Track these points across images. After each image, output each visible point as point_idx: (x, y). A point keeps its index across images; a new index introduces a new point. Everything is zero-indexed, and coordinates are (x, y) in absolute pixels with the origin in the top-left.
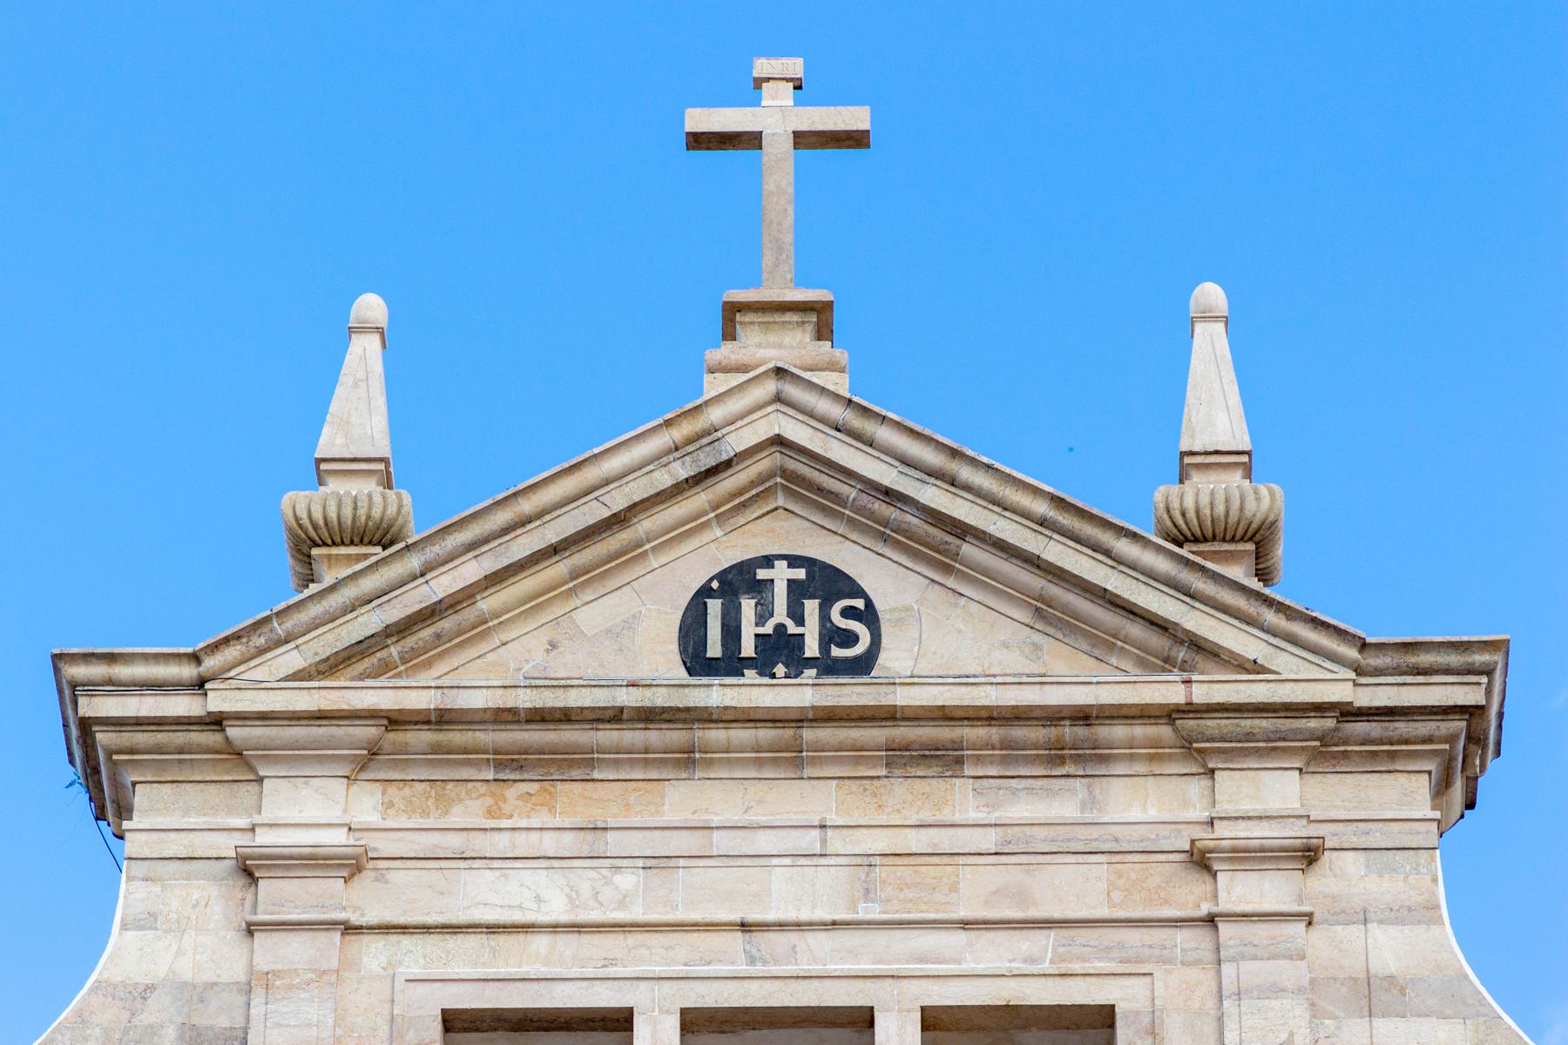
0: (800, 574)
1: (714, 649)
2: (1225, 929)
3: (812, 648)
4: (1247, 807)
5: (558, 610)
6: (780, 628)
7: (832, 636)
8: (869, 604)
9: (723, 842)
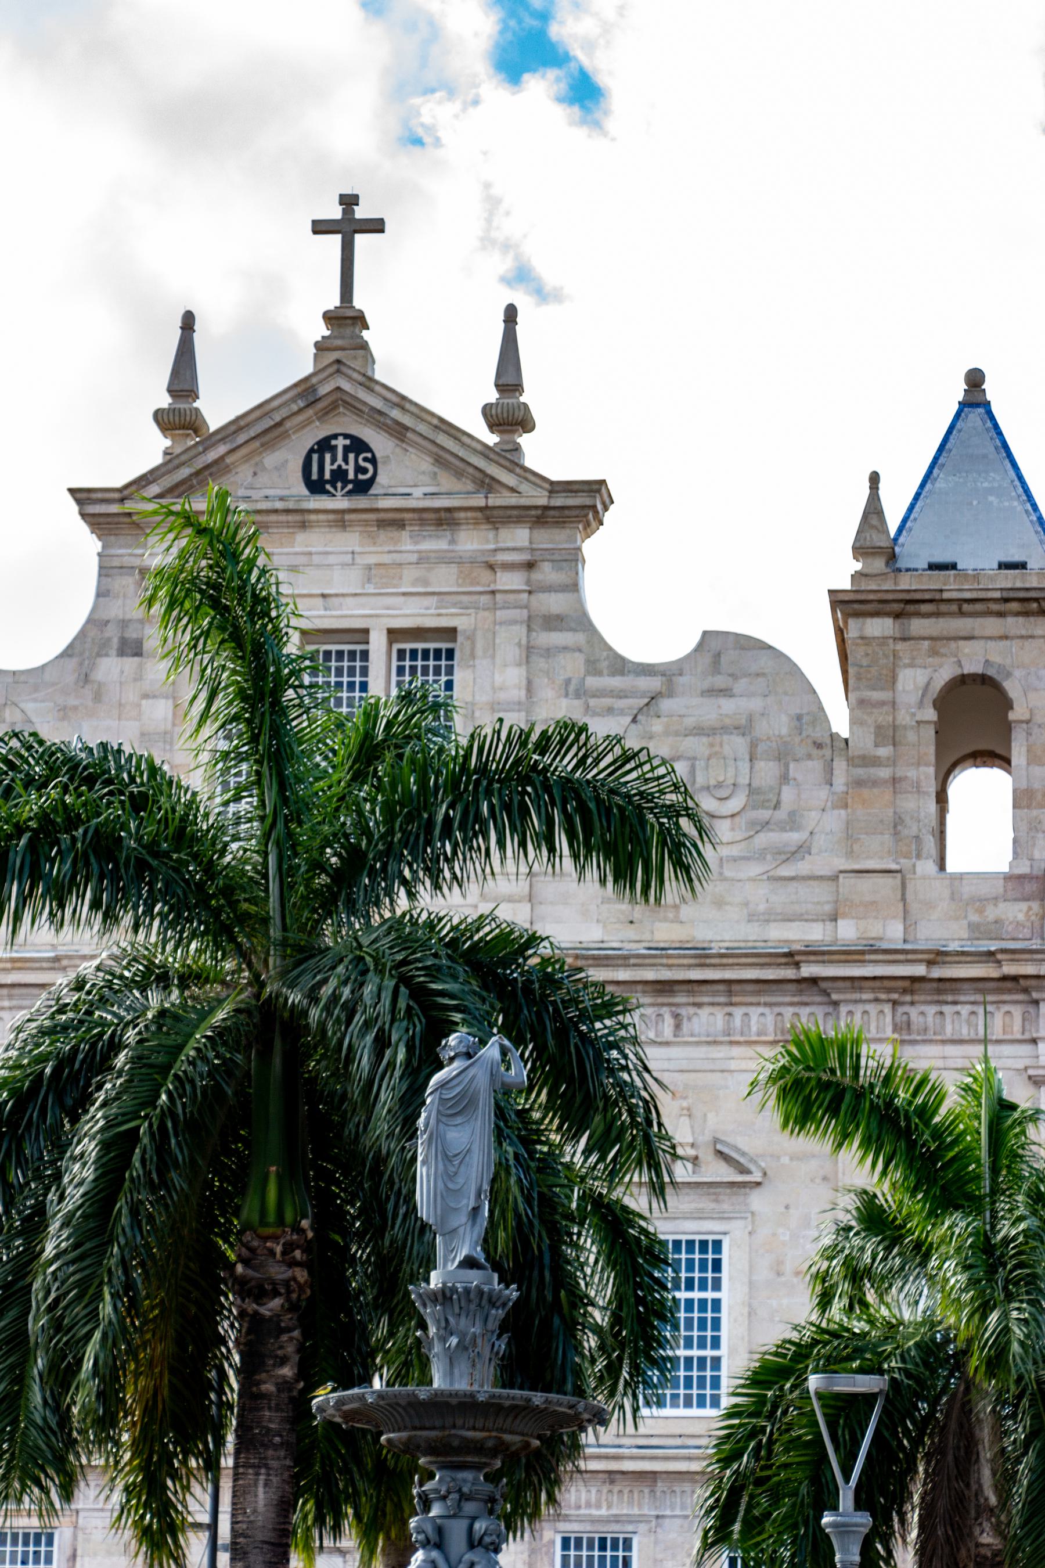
0: (348, 442)
1: (315, 476)
2: (498, 596)
3: (351, 476)
4: (510, 544)
5: (257, 459)
6: (340, 466)
7: (360, 470)
8: (374, 455)
9: (316, 559)
